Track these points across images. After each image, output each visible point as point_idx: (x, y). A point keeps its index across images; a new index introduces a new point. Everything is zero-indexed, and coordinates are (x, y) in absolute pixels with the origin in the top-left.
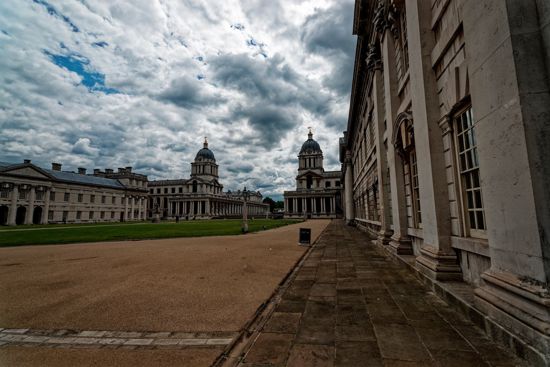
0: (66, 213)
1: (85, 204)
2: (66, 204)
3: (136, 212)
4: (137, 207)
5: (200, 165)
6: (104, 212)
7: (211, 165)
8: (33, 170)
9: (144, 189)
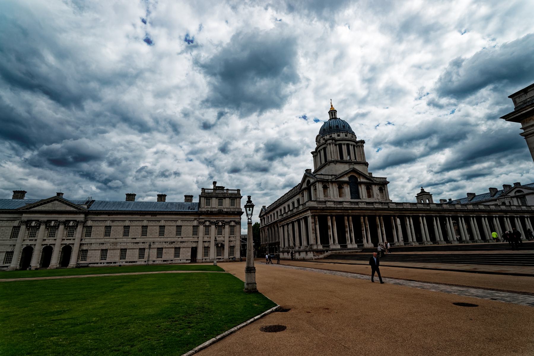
0: (104, 252)
1: (133, 238)
2: (106, 240)
3: (220, 247)
4: (222, 239)
5: (319, 151)
6: (162, 248)
7: (338, 142)
8: (60, 203)
9: (232, 210)
